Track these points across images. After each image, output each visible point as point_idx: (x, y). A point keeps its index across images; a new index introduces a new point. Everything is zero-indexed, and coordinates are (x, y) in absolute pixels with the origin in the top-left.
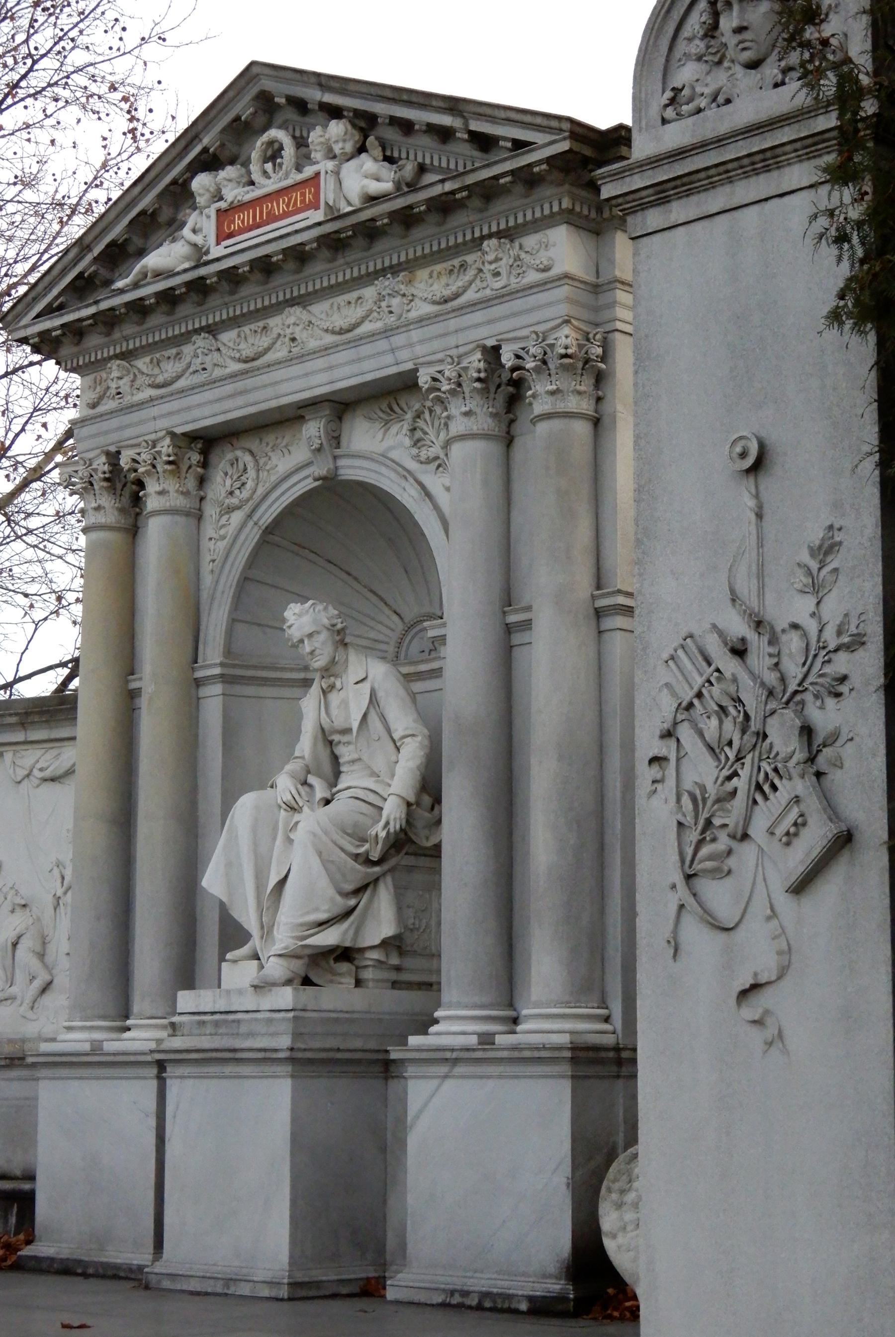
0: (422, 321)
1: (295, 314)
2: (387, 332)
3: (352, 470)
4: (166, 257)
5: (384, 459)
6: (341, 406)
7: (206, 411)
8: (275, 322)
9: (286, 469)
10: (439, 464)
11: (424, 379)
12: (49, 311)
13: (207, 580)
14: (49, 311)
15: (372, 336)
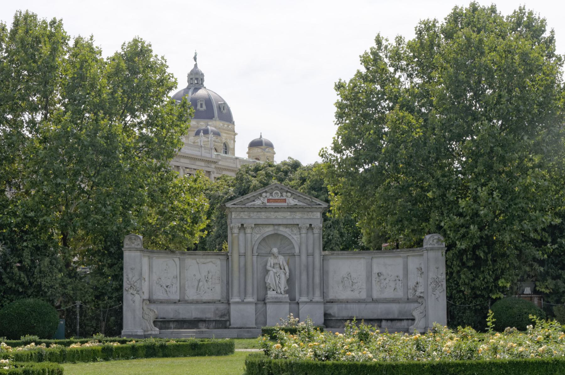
0: (298, 219)
1: (276, 214)
2: (293, 219)
3: (280, 233)
4: (258, 202)
5: (285, 232)
6: (280, 225)
7: (259, 222)
8: (272, 213)
9: (269, 231)
10: (296, 234)
11: (300, 226)
12: (234, 204)
13: (254, 243)
14: (234, 204)
15: (290, 219)
